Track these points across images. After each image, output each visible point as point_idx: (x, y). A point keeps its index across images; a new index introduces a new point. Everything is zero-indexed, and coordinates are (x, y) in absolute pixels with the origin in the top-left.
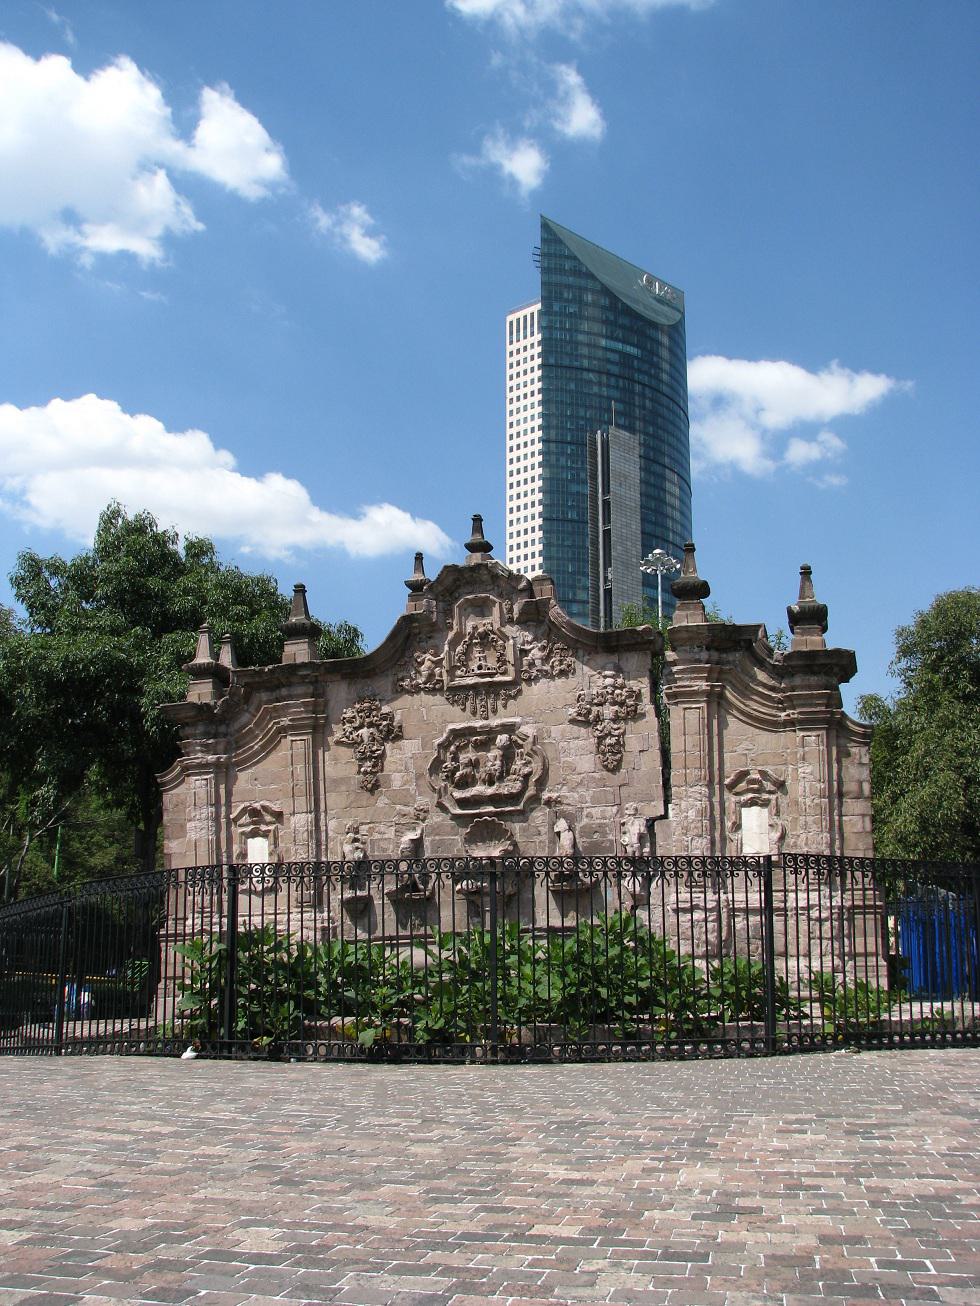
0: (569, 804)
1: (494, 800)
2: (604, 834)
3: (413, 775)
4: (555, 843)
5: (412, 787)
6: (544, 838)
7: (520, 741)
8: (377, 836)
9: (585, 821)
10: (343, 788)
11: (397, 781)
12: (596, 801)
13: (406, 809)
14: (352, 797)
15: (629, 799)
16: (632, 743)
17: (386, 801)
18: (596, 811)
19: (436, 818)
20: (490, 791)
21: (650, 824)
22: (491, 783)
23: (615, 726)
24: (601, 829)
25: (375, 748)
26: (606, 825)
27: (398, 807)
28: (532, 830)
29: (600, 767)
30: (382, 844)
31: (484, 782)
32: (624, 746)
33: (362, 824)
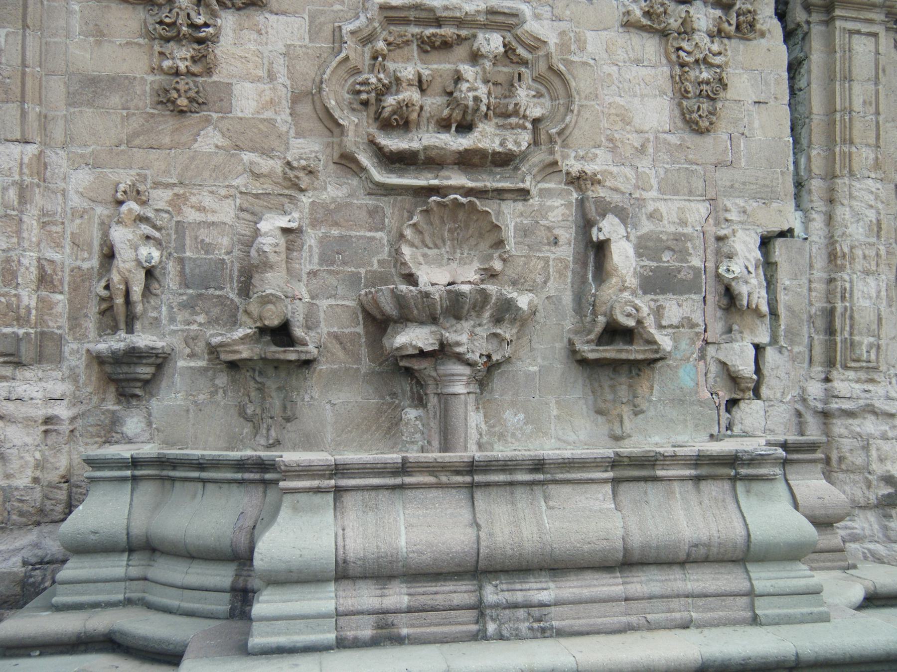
0: (615, 190)
1: (467, 161)
2: (683, 254)
3: (284, 94)
4: (585, 265)
5: (283, 118)
6: (566, 251)
7: (521, 51)
8: (191, 216)
9: (646, 227)
10: (115, 100)
11: (247, 100)
12: (669, 188)
13: (266, 165)
14: (135, 123)
15: (731, 190)
16: (742, 86)
17: (219, 140)
18: (670, 209)
19: (333, 189)
20: (463, 143)
21: (766, 242)
22: (465, 127)
23: (715, 48)
24: (678, 244)
25: (200, 20)
26: (687, 237)
27: (247, 157)
28: (542, 234)
29: (680, 124)
30: (203, 234)
31: (444, 125)
32: (725, 86)
33: (157, 185)
